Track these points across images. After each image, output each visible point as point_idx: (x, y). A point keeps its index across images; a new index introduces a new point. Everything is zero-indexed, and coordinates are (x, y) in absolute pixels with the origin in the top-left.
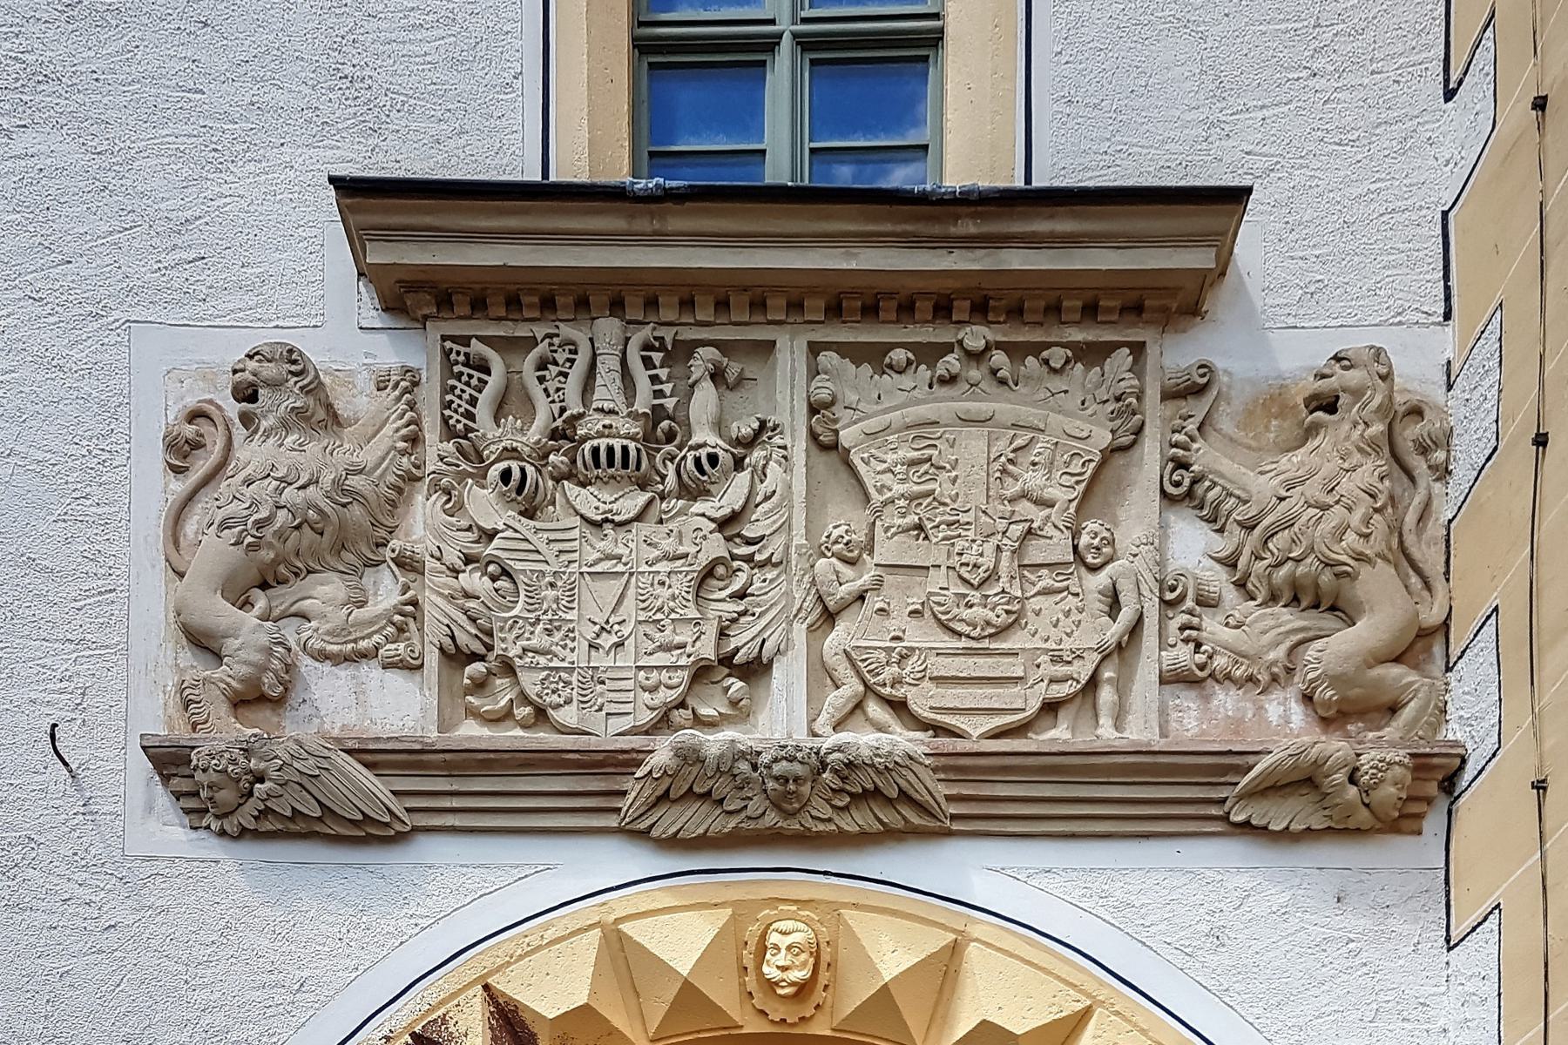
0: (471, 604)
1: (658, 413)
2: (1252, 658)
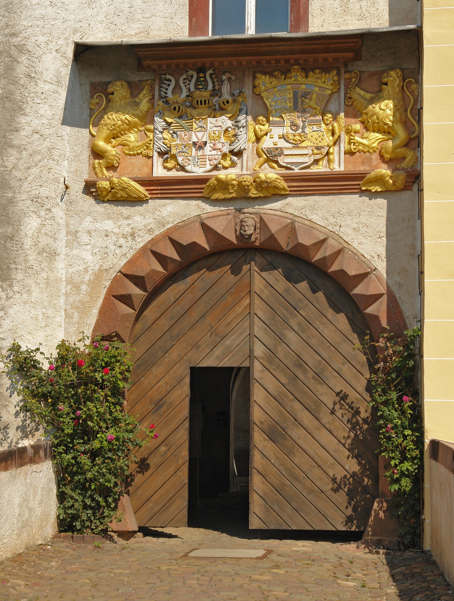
0: (165, 141)
1: (214, 90)
2: (368, 146)
